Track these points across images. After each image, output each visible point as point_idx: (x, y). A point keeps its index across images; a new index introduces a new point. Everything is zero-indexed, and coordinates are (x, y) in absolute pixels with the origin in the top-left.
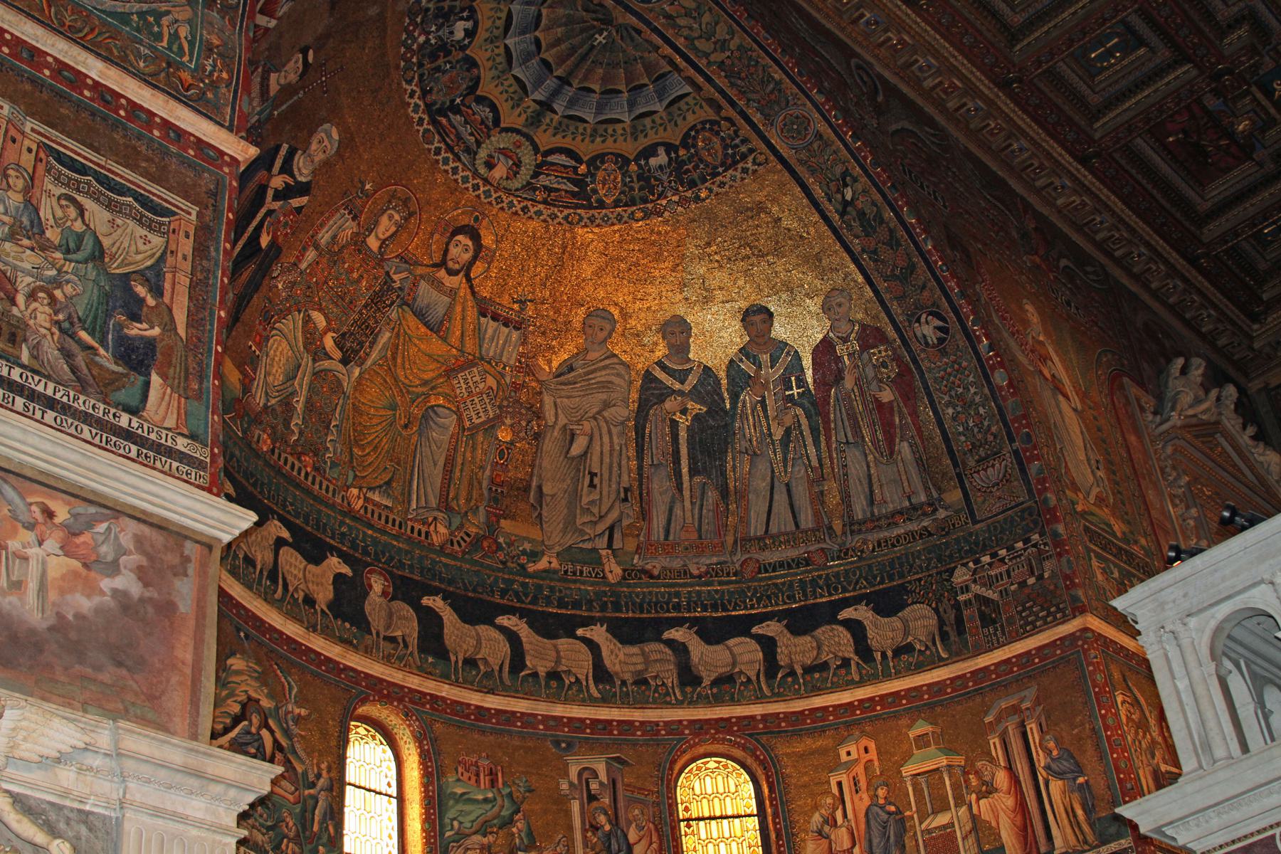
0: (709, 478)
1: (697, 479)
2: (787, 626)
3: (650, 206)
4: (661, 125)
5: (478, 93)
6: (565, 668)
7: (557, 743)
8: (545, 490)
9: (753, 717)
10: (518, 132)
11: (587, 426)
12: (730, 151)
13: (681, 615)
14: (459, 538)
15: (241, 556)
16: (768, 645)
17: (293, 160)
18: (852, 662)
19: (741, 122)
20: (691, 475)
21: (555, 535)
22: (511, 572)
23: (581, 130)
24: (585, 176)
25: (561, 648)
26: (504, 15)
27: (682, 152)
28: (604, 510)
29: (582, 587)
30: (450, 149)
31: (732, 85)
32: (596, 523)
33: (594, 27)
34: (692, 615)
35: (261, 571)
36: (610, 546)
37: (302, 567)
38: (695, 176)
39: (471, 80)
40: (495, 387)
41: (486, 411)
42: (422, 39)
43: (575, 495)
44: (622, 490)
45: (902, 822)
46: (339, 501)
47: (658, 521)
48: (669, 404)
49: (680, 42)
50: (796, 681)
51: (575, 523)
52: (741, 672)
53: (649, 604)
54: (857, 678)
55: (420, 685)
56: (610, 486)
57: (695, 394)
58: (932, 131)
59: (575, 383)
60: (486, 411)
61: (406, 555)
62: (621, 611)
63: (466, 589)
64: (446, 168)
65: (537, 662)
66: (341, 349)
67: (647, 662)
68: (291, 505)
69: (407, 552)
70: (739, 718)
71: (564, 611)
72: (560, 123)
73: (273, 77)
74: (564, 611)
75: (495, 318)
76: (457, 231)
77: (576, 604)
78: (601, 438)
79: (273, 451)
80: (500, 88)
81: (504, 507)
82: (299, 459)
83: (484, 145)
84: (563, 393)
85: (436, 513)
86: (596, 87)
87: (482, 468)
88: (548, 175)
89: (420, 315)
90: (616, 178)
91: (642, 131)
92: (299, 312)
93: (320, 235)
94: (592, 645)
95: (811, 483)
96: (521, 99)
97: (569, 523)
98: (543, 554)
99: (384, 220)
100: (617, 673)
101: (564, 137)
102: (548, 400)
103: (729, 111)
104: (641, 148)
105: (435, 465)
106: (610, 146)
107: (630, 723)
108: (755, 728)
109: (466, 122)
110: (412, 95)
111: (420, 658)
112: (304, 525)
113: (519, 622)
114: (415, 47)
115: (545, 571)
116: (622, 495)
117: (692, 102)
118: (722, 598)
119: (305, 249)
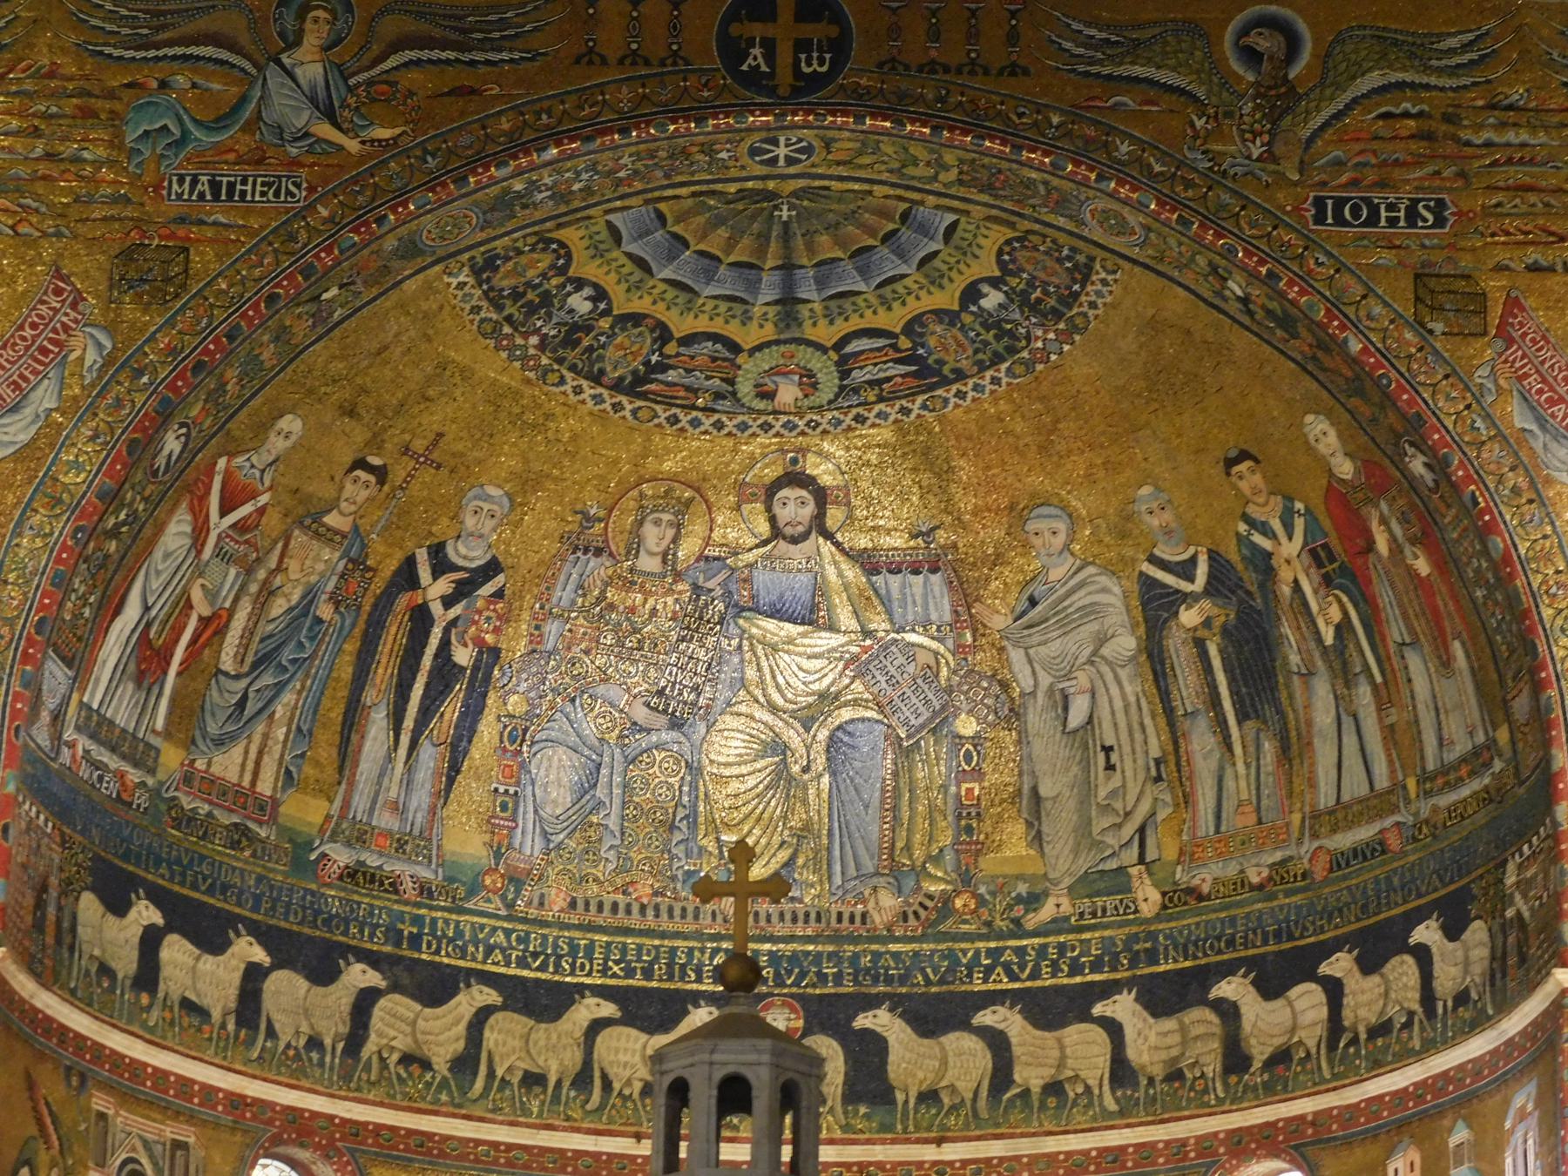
0: (1265, 722)
1: (1250, 725)
2: (1358, 960)
3: (1025, 354)
4: (958, 262)
5: (677, 335)
6: (1071, 1073)
8: (1043, 792)
9: (1302, 1118)
10: (777, 342)
11: (1083, 679)
12: (1069, 265)
13: (1235, 955)
14: (916, 907)
15: (515, 1079)
16: (1334, 990)
17: (446, 556)
18: (1416, 1019)
19: (1048, 231)
20: (1239, 723)
21: (1065, 862)
22: (1000, 936)
23: (863, 304)
24: (914, 348)
25: (1067, 1041)
26: (624, 260)
27: (1014, 282)
28: (1131, 799)
29: (1107, 933)
30: (694, 407)
31: (996, 197)
32: (1119, 826)
33: (763, 209)
34: (1251, 952)
35: (559, 1083)
36: (1141, 859)
37: (638, 1046)
38: (1052, 302)
39: (652, 331)
40: (932, 663)
41: (927, 702)
42: (534, 340)
43: (1086, 788)
44: (1152, 764)
46: (709, 920)
48: (1189, 617)
49: (885, 176)
50: (1357, 1054)
51: (1090, 833)
52: (1300, 1042)
53: (1196, 944)
54: (1416, 1043)
55: (839, 1155)
56: (1135, 761)
57: (1211, 590)
58: (1471, 36)
59: (1047, 620)
60: (927, 702)
61: (829, 960)
62: (1157, 963)
63: (928, 982)
64: (702, 428)
65: (1029, 1076)
66: (665, 711)
68: (617, 962)
69: (831, 955)
70: (1289, 1120)
71: (1078, 979)
72: (826, 308)
73: (331, 520)
74: (1078, 979)
75: (895, 570)
77: (1096, 966)
78: (1107, 690)
79: (573, 904)
80: (703, 319)
81: (982, 837)
82: (624, 893)
83: (739, 379)
84: (1036, 639)
85: (875, 880)
86: (840, 254)
87: (944, 788)
88: (861, 368)
89: (776, 613)
90: (955, 338)
91: (942, 276)
92: (573, 700)
93: (554, 600)
94: (1113, 1029)
95: (1379, 709)
96: (746, 312)
97: (1084, 835)
98: (1046, 894)
100: (1143, 1067)
101: (846, 319)
102: (1016, 656)
103: (1027, 225)
104: (957, 294)
105: (867, 807)
106: (914, 307)
107: (1152, 1145)
108: (1303, 1134)
109: (688, 371)
110: (578, 390)
111: (845, 1113)
112: (644, 983)
113: (1008, 1014)
114: (532, 351)
115: (1054, 921)
116: (1154, 772)
117: (971, 227)
118: (1287, 921)
119: (537, 628)
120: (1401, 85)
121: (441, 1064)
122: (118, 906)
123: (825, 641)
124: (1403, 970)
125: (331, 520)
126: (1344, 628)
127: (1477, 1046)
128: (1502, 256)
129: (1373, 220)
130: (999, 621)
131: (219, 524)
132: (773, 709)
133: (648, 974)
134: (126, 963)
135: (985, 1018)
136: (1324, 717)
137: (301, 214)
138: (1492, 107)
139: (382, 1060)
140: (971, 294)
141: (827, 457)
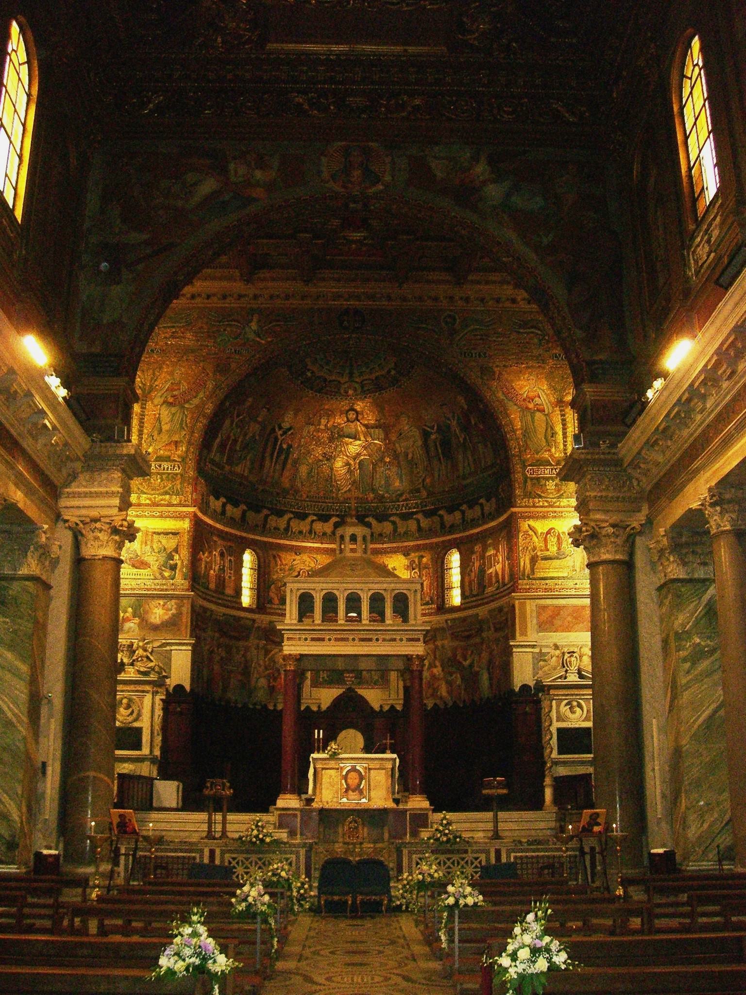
7: (404, 555)
16: (463, 512)
36: (423, 486)
45: (485, 571)
47: (436, 475)
48: (433, 437)
57: (436, 432)
65: (401, 530)
67: (433, 522)
75: (373, 428)
76: (347, 414)
77: (414, 508)
79: (307, 497)
94: (418, 521)
95: (472, 456)
99: (322, 421)
102: (397, 445)
106: (377, 374)
120: (476, 329)
121: (282, 530)
122: (217, 498)
123: (358, 442)
124: (477, 508)
125: (259, 419)
126: (465, 439)
127: (493, 524)
128: (498, 364)
129: (472, 356)
130: (394, 439)
131: (236, 420)
132: (347, 456)
133: (323, 511)
134: (219, 510)
135: (392, 519)
136: (460, 457)
137: (253, 357)
138: (495, 333)
139: (270, 530)
140: (389, 372)
141: (359, 405)
